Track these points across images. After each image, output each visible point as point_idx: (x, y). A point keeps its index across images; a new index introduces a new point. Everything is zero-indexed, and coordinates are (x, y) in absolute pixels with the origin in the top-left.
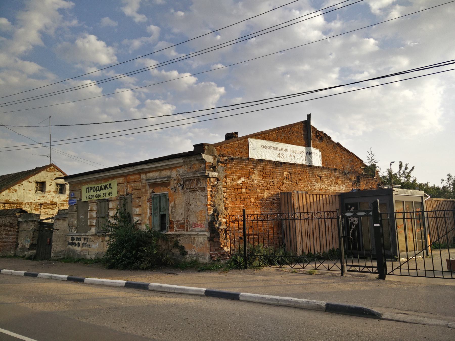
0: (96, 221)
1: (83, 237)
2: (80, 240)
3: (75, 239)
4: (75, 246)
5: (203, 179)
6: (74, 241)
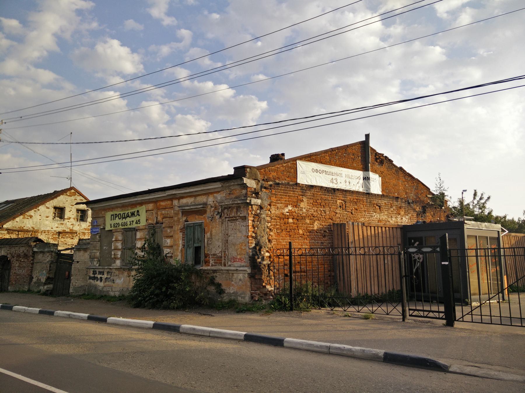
2: (103, 274)
3: (97, 273)
4: (97, 281)
5: (244, 207)
6: (96, 276)
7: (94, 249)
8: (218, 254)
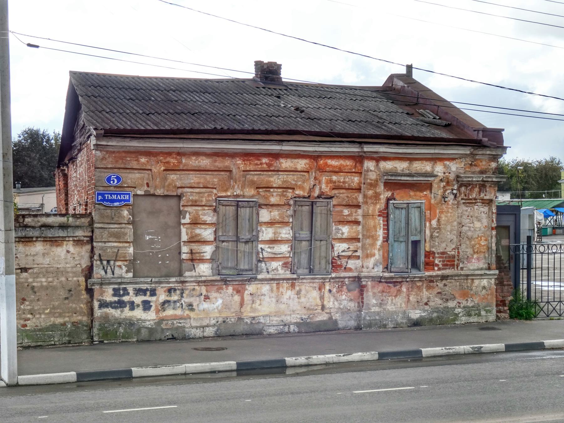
0: (214, 249)
1: (162, 287)
3: (131, 292)
5: (490, 186)
6: (126, 298)
7: (111, 239)
8: (450, 252)
